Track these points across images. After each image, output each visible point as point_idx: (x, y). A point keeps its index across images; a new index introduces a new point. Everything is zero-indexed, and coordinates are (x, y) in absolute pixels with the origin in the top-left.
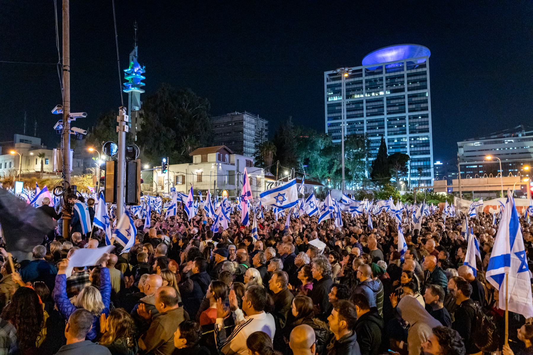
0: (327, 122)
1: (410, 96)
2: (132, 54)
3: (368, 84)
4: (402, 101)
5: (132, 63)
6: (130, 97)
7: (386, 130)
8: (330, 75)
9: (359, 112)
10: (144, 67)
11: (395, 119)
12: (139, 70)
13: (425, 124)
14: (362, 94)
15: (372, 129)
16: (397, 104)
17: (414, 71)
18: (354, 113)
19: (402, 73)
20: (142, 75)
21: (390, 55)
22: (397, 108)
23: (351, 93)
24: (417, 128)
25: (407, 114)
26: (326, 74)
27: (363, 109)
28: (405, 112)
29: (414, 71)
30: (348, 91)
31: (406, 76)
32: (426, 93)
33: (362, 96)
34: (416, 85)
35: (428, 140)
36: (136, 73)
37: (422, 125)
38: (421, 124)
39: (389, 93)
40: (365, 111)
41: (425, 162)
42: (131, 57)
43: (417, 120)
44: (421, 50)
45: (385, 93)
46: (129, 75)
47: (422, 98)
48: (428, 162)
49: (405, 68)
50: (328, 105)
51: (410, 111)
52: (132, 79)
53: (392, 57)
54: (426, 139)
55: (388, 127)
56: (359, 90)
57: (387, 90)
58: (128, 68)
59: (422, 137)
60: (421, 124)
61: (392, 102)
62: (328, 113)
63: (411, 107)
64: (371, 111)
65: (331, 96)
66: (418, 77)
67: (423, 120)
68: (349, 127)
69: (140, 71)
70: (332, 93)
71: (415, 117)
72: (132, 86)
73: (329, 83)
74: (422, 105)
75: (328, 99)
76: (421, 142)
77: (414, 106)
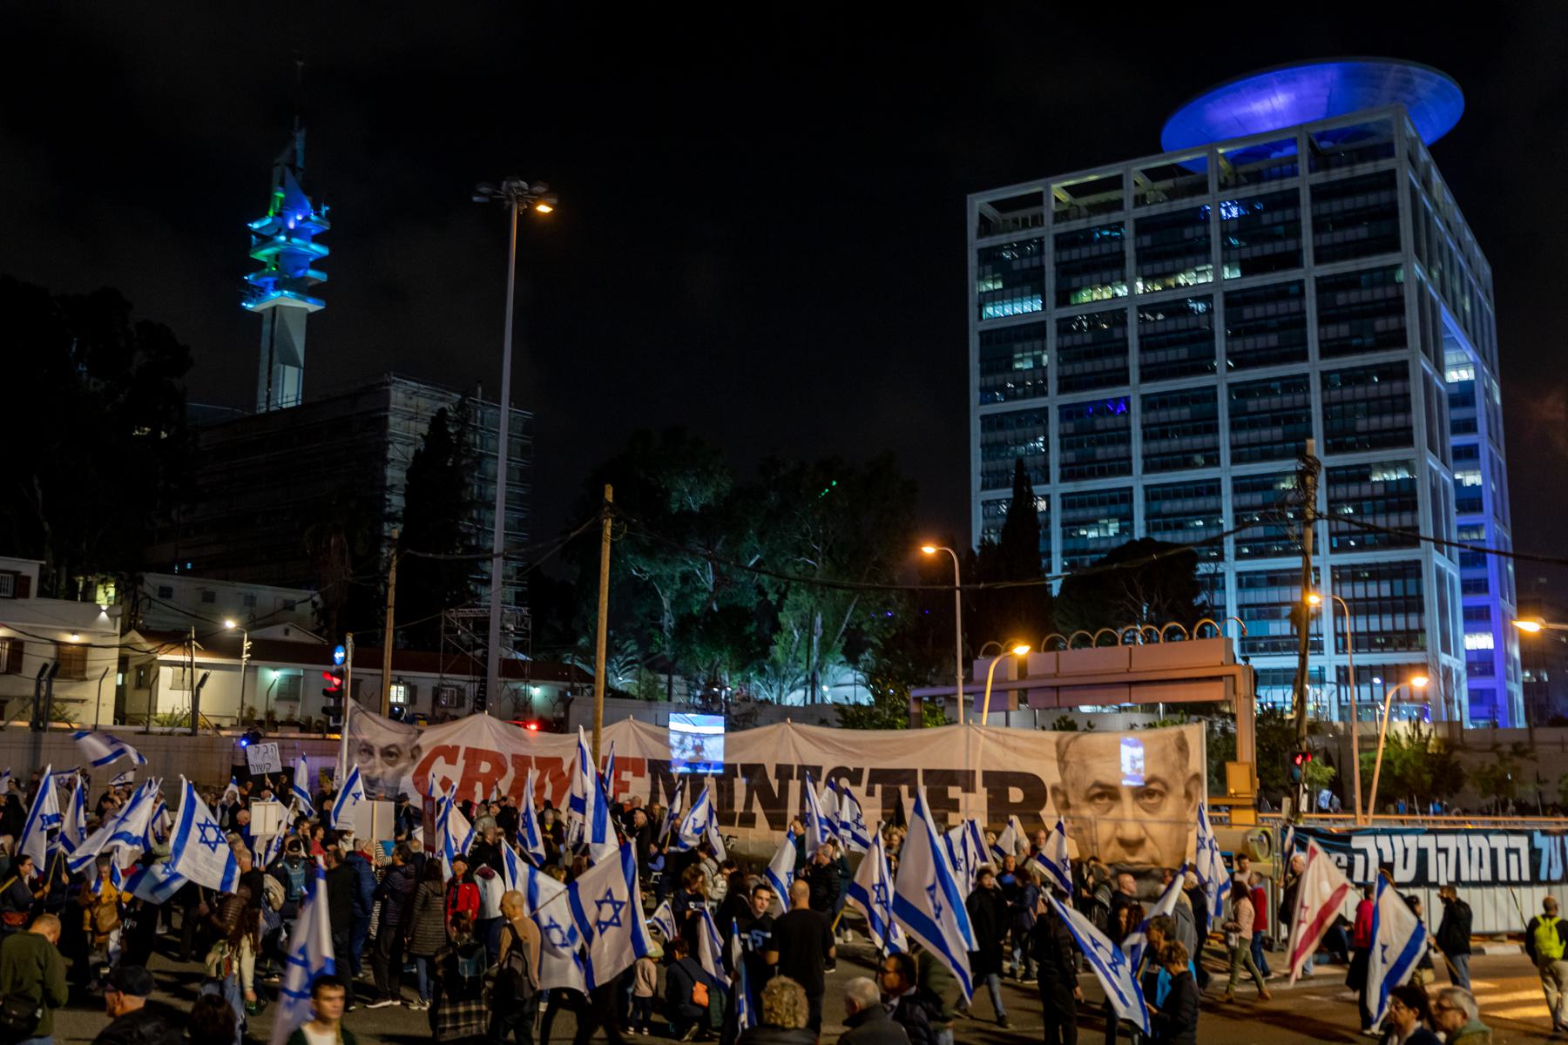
0: (977, 411)
1: (1323, 285)
2: (284, 157)
3: (1147, 240)
4: (1294, 306)
5: (280, 195)
6: (266, 327)
7: (1224, 438)
8: (999, 205)
9: (1108, 363)
10: (324, 209)
11: (1264, 388)
12: (306, 219)
13: (1393, 411)
14: (1123, 280)
15: (1164, 435)
16: (1273, 323)
17: (1338, 174)
18: (1088, 366)
19: (1288, 184)
20: (316, 239)
21: (1271, 105)
22: (1273, 340)
23: (1075, 282)
24: (1361, 424)
25: (1314, 366)
26: (978, 203)
27: (1124, 351)
28: (1303, 357)
29: (1338, 174)
30: (1064, 270)
31: (1305, 197)
32: (1396, 267)
33: (1122, 291)
34: (1350, 234)
35: (1412, 482)
36: (290, 234)
37: (1381, 413)
38: (1377, 407)
39: (1237, 274)
40: (1134, 359)
41: (1398, 583)
42: (277, 172)
43: (1360, 391)
44: (1409, 81)
45: (1217, 273)
46: (266, 240)
47: (1379, 293)
48: (1411, 582)
49: (1303, 165)
50: (982, 333)
51: (1327, 351)
52: (277, 257)
53: (1274, 115)
54: (1403, 474)
55: (1235, 427)
56: (1109, 267)
57: (1226, 261)
58: (262, 214)
59: (1384, 466)
60: (1377, 407)
61: (1248, 313)
62: (983, 373)
63: (1332, 331)
64: (1161, 356)
65: (993, 297)
66: (1360, 201)
67: (1385, 389)
68: (1070, 427)
69: (306, 225)
70: (999, 285)
71: (1353, 377)
72: (278, 286)
73: (986, 242)
74: (1380, 324)
75: (981, 307)
76: (1380, 490)
77: (1344, 330)
